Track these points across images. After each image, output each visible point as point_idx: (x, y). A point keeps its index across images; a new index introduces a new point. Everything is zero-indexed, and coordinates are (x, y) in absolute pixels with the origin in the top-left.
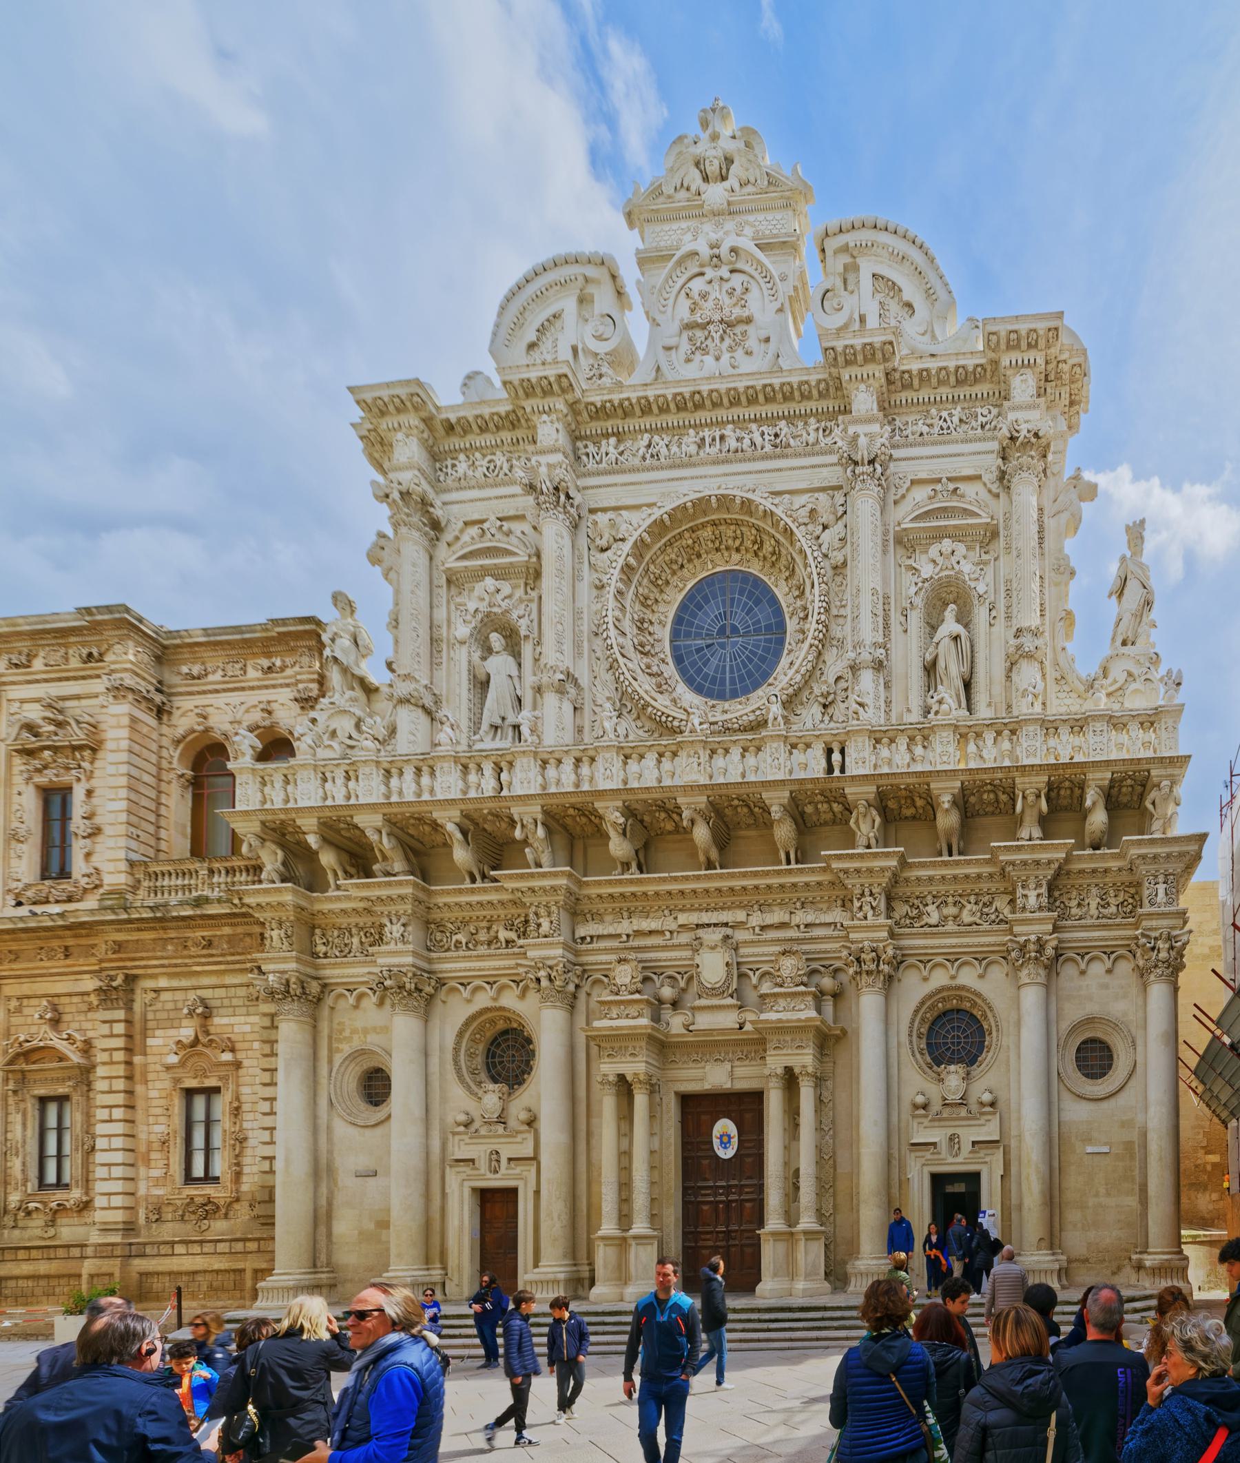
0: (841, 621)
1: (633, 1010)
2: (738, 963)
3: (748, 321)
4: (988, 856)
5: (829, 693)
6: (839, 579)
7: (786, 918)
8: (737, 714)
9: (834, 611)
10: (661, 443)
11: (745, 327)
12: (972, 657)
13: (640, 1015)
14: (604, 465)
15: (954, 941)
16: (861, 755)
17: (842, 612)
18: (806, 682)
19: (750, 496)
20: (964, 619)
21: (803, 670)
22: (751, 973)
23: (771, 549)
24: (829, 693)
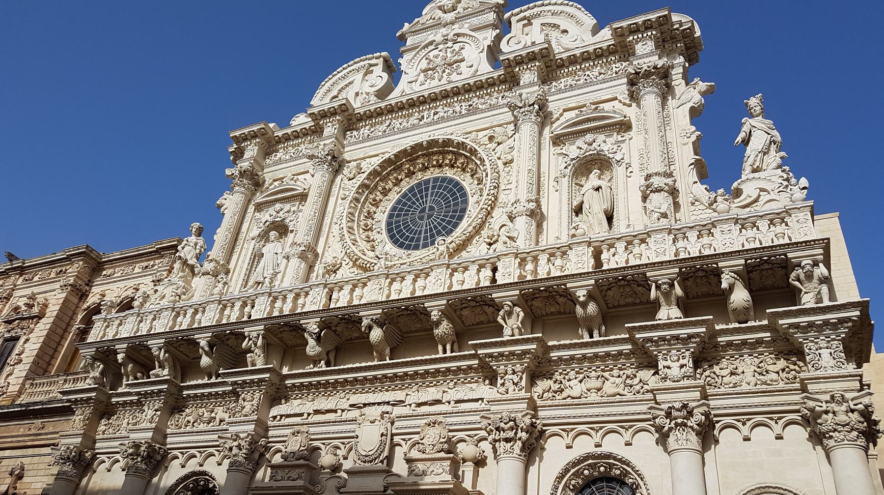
1: (294, 474)
2: (393, 435)
3: (462, 60)
4: (627, 336)
5: (493, 236)
7: (439, 397)
8: (421, 257)
9: (502, 187)
11: (459, 64)
13: (299, 478)
15: (597, 411)
16: (508, 270)
17: (508, 187)
21: (474, 224)
22: (403, 443)
24: (493, 236)
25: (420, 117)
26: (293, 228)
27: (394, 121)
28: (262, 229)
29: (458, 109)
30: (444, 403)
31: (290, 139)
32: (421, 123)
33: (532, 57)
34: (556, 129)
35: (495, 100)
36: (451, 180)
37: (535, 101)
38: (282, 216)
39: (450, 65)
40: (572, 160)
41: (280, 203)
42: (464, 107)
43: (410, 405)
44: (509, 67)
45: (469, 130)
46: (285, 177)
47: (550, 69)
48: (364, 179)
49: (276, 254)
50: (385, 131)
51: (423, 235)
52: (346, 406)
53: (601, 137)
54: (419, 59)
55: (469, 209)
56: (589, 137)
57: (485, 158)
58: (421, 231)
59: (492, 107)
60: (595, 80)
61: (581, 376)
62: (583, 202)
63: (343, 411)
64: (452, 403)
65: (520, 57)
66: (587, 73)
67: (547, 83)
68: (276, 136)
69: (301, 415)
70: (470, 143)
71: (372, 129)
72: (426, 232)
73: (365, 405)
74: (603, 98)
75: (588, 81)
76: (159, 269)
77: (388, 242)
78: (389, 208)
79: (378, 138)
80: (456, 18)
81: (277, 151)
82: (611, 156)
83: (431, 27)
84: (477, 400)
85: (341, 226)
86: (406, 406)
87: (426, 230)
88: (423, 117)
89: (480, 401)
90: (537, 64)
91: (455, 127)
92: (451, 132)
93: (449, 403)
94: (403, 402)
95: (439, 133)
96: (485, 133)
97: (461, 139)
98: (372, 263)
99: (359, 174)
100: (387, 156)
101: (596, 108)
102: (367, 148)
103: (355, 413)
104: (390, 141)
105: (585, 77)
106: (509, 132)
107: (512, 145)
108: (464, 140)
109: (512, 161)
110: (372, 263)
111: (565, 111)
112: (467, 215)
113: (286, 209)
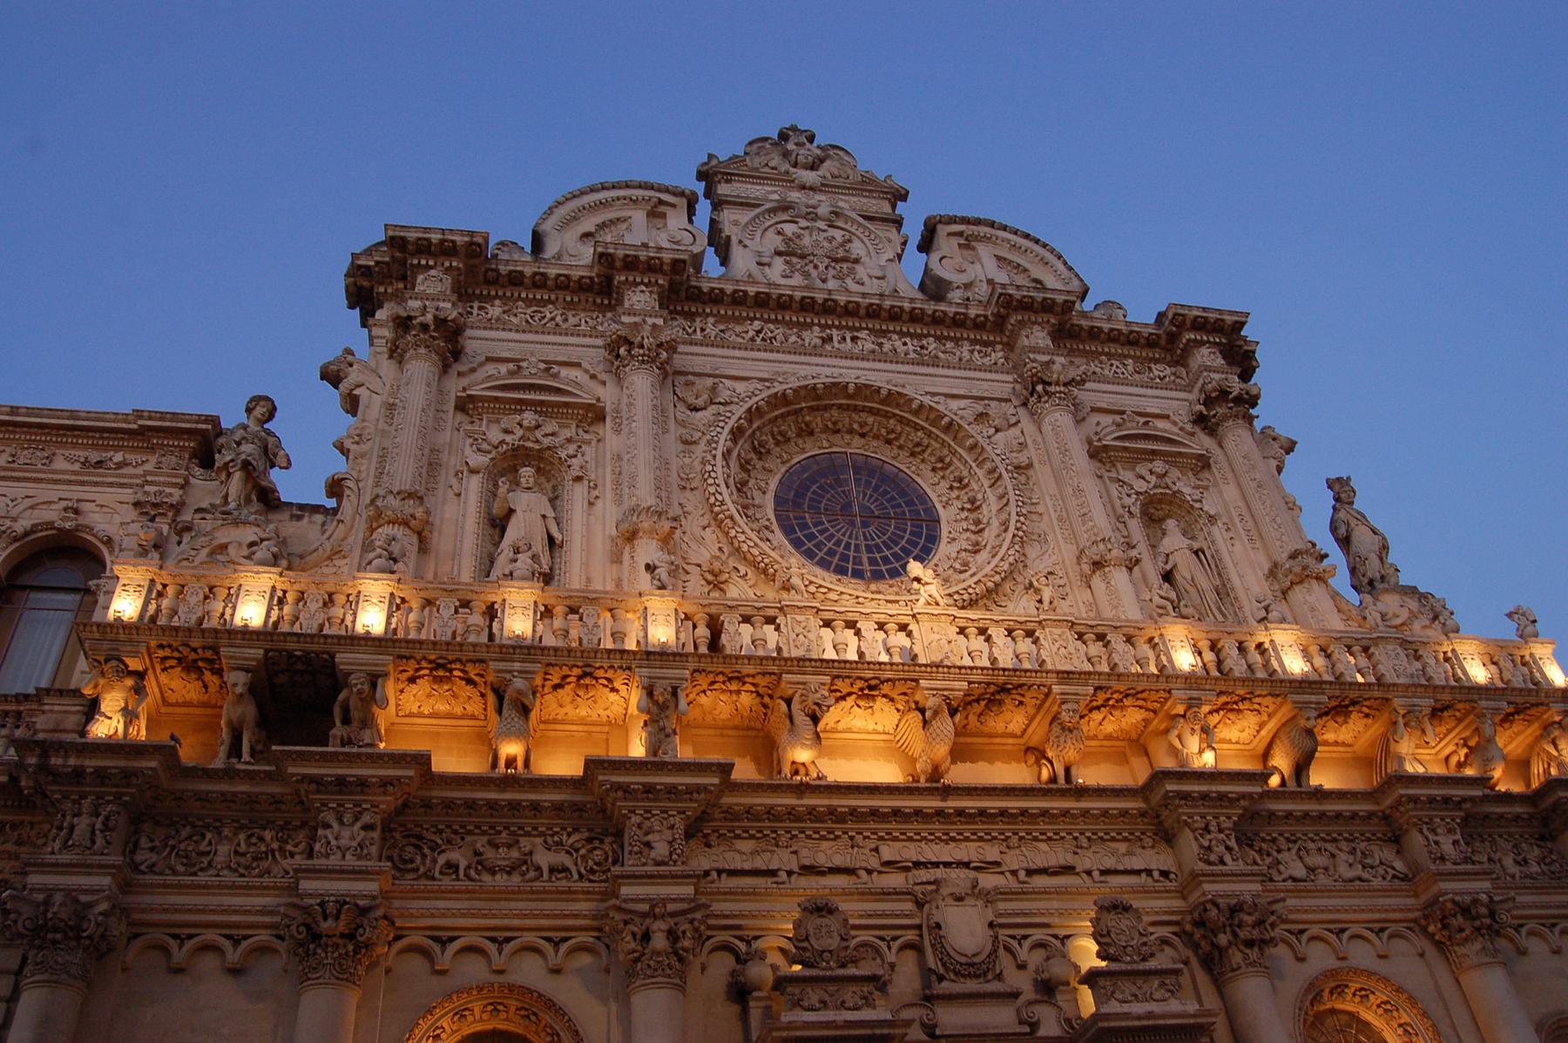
0: (1034, 517)
19: (900, 390)
25: (824, 335)
27: (772, 326)
28: (490, 456)
30: (1077, 874)
31: (521, 284)
32: (828, 347)
34: (1105, 435)
35: (966, 355)
37: (1073, 380)
38: (547, 441)
39: (836, 260)
40: (1137, 493)
41: (536, 412)
43: (1014, 873)
46: (524, 360)
49: (544, 517)
50: (752, 339)
52: (874, 863)
53: (1175, 473)
54: (763, 227)
56: (1159, 466)
59: (961, 365)
61: (1297, 846)
62: (1175, 566)
63: (869, 872)
64: (1096, 874)
68: (492, 270)
69: (772, 873)
71: (722, 327)
73: (917, 865)
74: (1149, 410)
76: (149, 478)
77: (793, 551)
78: (773, 484)
80: (822, 185)
81: (489, 299)
82: (1197, 505)
83: (764, 178)
84: (1137, 872)
86: (1002, 873)
88: (830, 339)
89: (1144, 875)
90: (1053, 321)
92: (901, 382)
93: (1089, 873)
94: (997, 864)
95: (879, 376)
97: (927, 400)
98: (821, 586)
99: (712, 403)
100: (778, 388)
101: (1147, 423)
103: (895, 880)
109: (1030, 466)
110: (821, 586)
112: (944, 540)
113: (548, 429)
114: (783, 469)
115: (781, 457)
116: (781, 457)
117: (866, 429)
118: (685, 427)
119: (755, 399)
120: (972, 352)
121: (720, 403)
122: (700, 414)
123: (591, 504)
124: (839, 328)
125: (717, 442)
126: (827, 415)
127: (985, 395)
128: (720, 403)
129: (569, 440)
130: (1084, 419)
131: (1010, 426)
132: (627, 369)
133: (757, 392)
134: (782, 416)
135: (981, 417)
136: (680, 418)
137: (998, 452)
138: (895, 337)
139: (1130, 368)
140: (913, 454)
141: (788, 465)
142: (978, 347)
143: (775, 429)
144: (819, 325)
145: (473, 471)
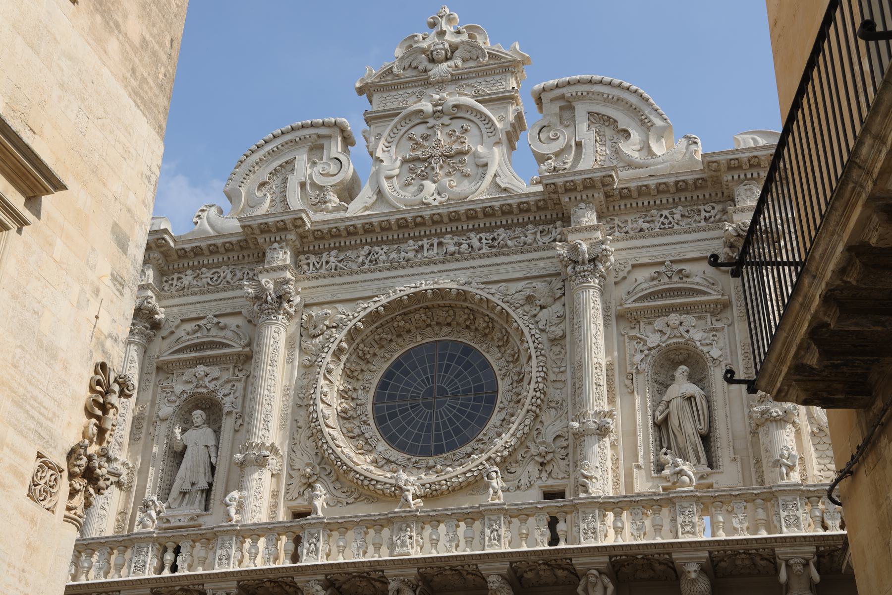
6: (556, 349)
10: (381, 252)
12: (710, 412)
14: (323, 271)
18: (522, 443)
20: (698, 377)
23: (484, 325)
26: (232, 409)
27: (376, 249)
28: (177, 404)
29: (475, 242)
32: (419, 256)
33: (589, 184)
36: (468, 350)
42: (484, 241)
44: (554, 193)
45: (494, 278)
47: (611, 199)
48: (341, 341)
49: (207, 446)
51: (433, 433)
55: (499, 400)
57: (526, 330)
58: (429, 425)
60: (675, 225)
65: (572, 184)
66: (665, 213)
67: (605, 217)
70: (500, 303)
72: (438, 429)
75: (667, 226)
77: (380, 438)
78: (375, 382)
79: (352, 273)
85: (315, 415)
87: (437, 425)
91: (473, 270)
96: (520, 285)
97: (485, 295)
100: (373, 307)
102: (336, 287)
104: (373, 280)
105: (662, 219)
106: (556, 291)
107: (562, 313)
108: (490, 297)
111: (633, 266)
112: (497, 409)
114: (386, 366)
115: (384, 357)
116: (384, 357)
117: (449, 320)
118: (306, 353)
119: (354, 322)
120: (535, 233)
121: (333, 327)
122: (317, 340)
123: (236, 431)
124: (428, 237)
125: (320, 367)
126: (417, 316)
127: (541, 273)
128: (333, 327)
129: (227, 382)
130: (624, 278)
131: (555, 300)
132: (260, 320)
133: (356, 314)
134: (382, 325)
135: (529, 299)
136: (302, 346)
137: (533, 332)
138: (472, 235)
139: (677, 217)
140: (485, 335)
141: (390, 362)
142: (541, 228)
143: (377, 337)
144: (412, 238)
145: (163, 420)
